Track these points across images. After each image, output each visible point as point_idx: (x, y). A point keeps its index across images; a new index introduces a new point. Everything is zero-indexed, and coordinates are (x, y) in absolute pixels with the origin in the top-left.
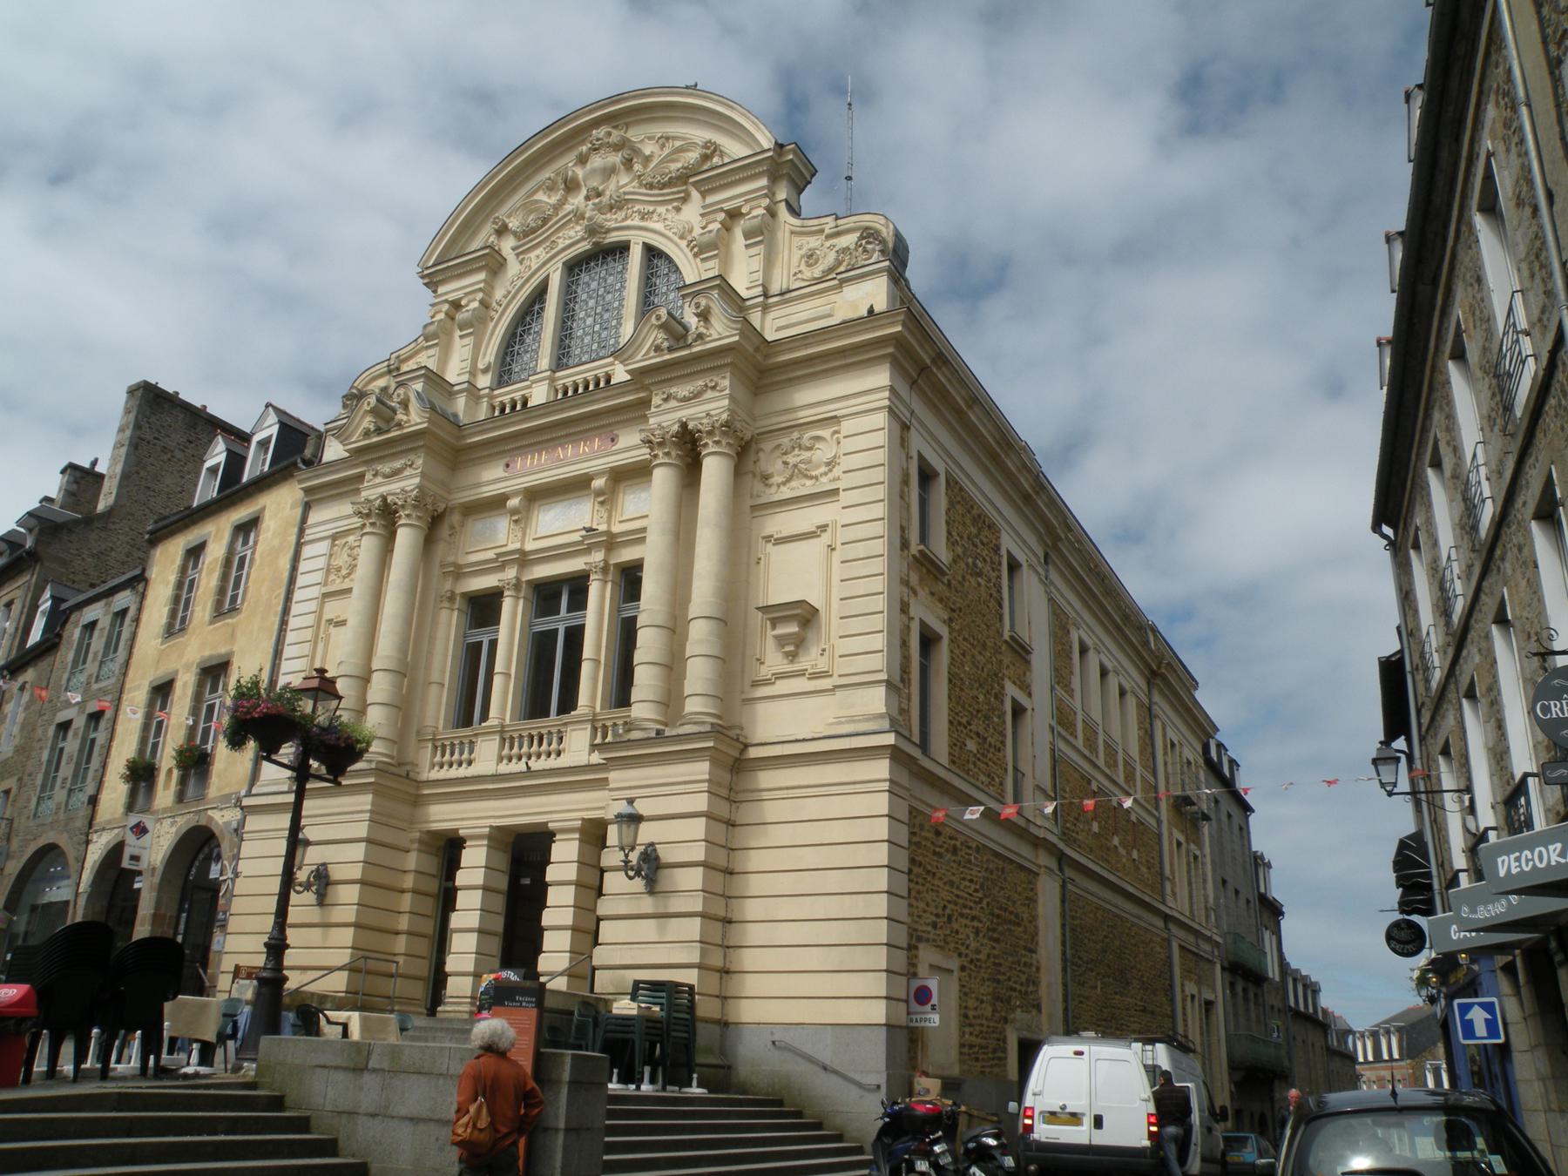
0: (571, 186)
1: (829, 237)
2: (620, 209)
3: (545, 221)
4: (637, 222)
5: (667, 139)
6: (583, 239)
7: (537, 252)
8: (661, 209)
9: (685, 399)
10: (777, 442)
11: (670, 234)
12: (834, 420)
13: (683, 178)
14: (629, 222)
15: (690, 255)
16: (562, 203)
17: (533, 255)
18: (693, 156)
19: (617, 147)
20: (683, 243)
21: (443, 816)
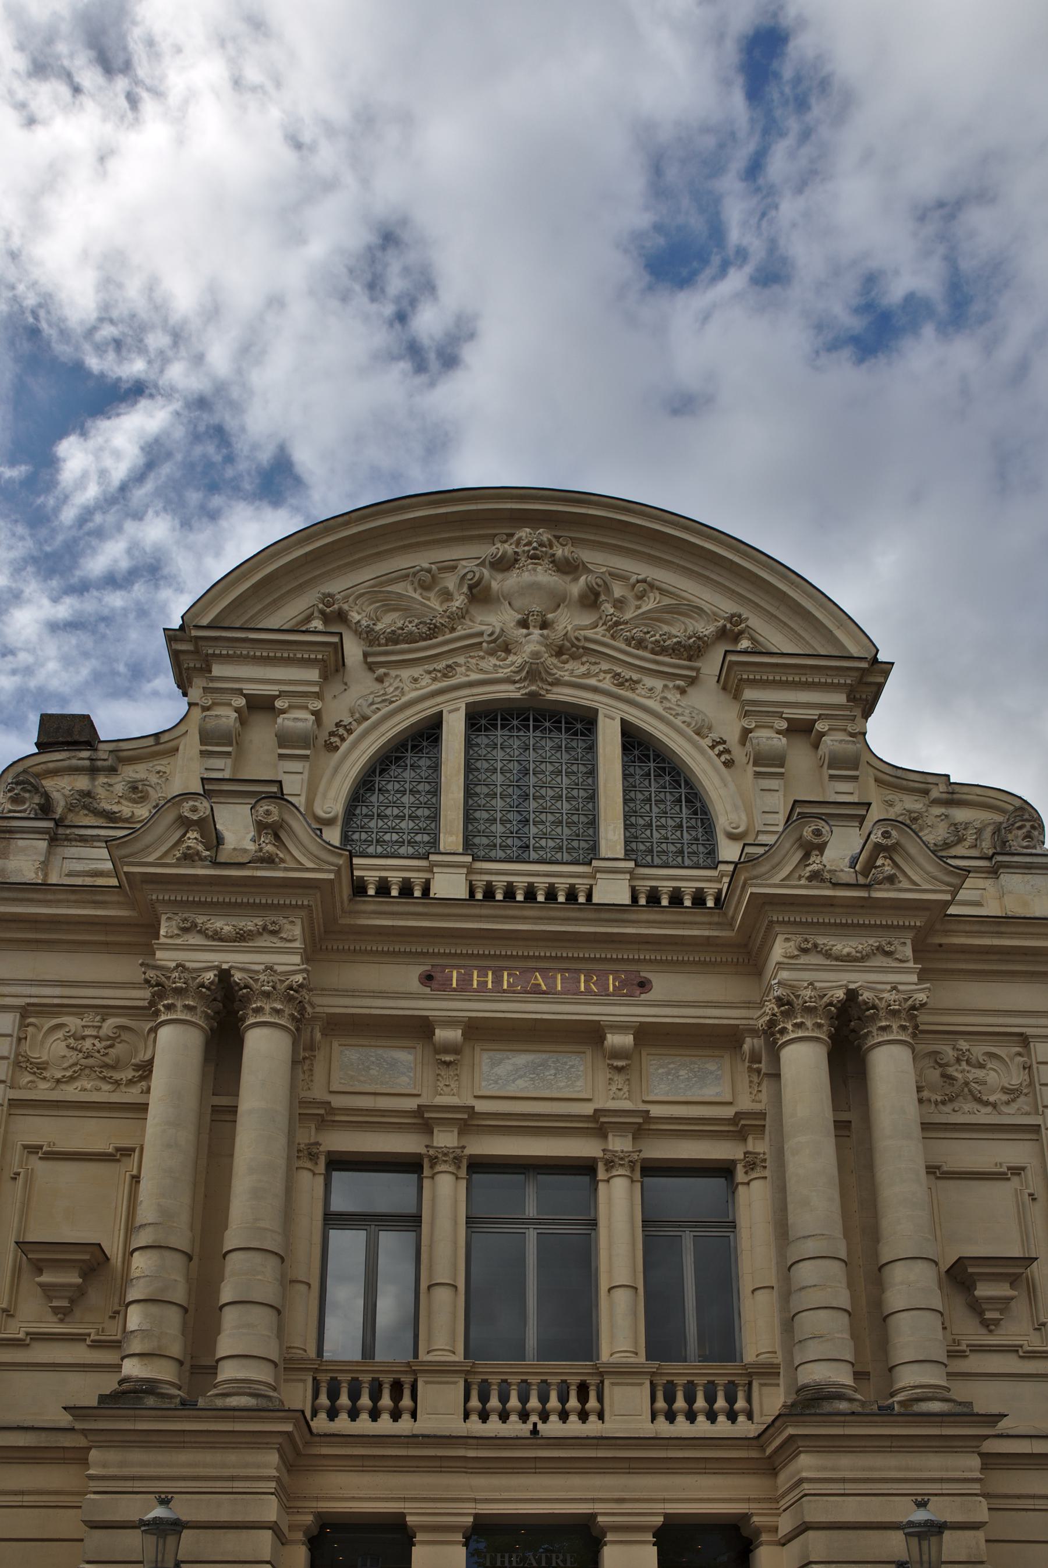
0: (479, 595)
1: (936, 802)
2: (574, 657)
3: (434, 631)
4: (607, 684)
5: (652, 586)
6: (508, 680)
7: (416, 671)
8: (649, 682)
9: (848, 958)
10: (937, 1048)
11: (678, 722)
12: (1024, 1040)
13: (693, 650)
14: (593, 682)
15: (719, 763)
16: (462, 615)
17: (406, 673)
18: (706, 629)
19: (568, 568)
20: (705, 743)
21: (358, 1493)
